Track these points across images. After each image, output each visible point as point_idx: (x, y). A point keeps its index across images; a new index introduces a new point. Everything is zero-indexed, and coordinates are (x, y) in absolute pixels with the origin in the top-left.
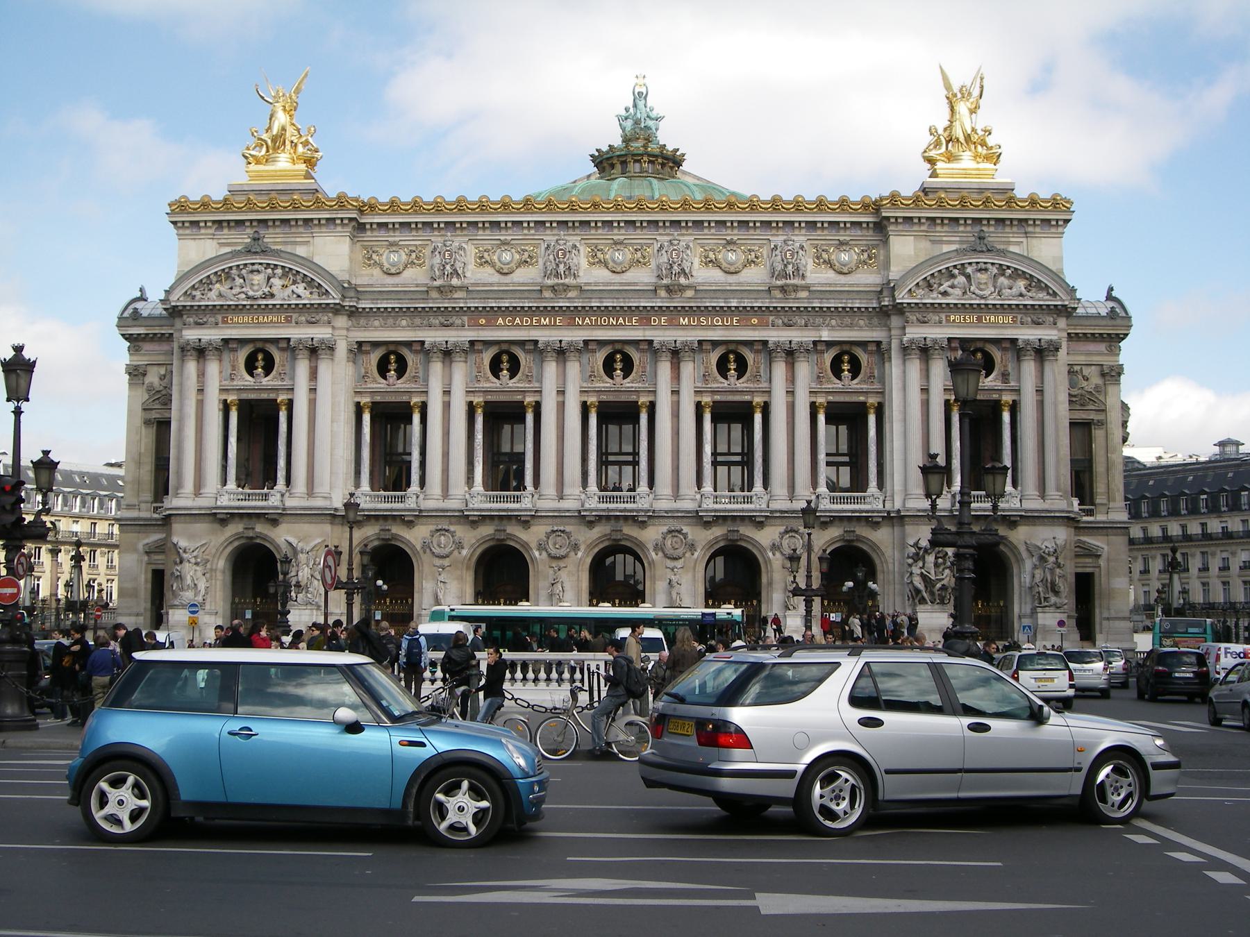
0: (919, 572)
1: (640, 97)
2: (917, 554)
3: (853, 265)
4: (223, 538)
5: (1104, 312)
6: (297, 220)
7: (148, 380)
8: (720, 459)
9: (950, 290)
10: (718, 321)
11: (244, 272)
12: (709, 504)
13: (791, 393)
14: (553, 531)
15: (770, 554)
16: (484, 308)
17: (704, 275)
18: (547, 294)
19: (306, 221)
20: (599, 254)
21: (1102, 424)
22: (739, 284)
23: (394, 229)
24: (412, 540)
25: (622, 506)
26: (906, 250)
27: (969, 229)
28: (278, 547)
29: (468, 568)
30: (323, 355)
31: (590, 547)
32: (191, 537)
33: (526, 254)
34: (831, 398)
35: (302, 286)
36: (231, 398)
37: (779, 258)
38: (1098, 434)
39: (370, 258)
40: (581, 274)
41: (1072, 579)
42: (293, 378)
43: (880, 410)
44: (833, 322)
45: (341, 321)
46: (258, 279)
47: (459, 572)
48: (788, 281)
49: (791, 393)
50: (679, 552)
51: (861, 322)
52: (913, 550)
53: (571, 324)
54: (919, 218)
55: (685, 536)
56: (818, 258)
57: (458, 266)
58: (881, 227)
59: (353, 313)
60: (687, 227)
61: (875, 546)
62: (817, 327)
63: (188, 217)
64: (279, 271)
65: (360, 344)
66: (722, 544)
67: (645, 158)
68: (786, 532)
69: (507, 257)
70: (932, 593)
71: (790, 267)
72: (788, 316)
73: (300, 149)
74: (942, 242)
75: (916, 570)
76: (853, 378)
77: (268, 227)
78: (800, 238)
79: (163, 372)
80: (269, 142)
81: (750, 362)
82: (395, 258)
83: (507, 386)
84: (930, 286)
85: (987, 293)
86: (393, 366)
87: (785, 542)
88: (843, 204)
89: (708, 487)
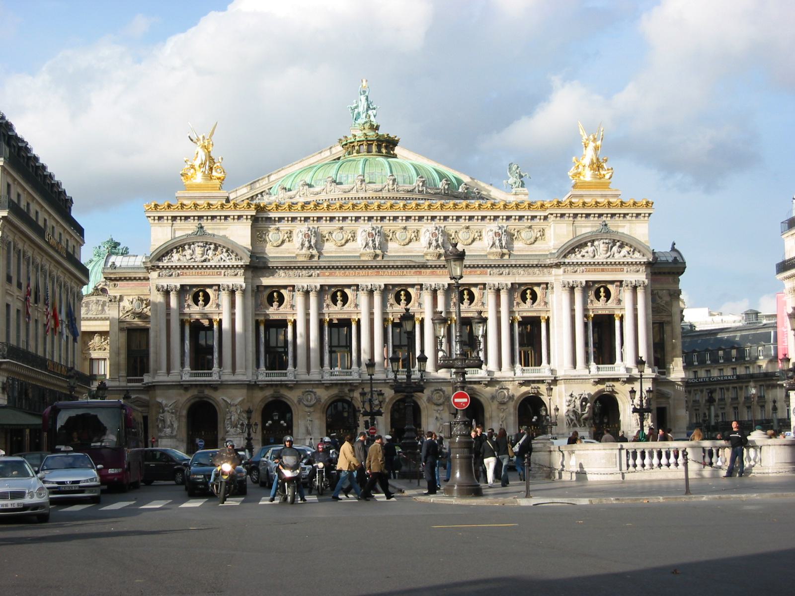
0: (572, 410)
5: (670, 260)
7: (122, 304)
9: (586, 254)
11: (192, 246)
15: (490, 401)
19: (226, 217)
21: (670, 323)
24: (292, 397)
27: (596, 219)
29: (323, 413)
35: (226, 254)
38: (667, 328)
39: (261, 238)
41: (655, 411)
45: (249, 274)
50: (441, 401)
53: (378, 275)
55: (444, 392)
58: (546, 218)
65: (258, 287)
67: (375, 143)
70: (579, 421)
74: (581, 226)
79: (131, 298)
80: (197, 167)
85: (608, 255)
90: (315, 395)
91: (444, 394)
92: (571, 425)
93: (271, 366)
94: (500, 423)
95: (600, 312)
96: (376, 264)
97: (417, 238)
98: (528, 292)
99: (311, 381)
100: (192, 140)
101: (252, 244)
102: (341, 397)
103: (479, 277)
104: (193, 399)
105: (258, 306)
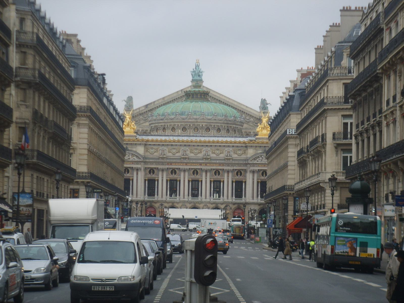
1: (197, 66)
10: (215, 165)
12: (212, 200)
13: (228, 179)
18: (182, 159)
19: (135, 144)
22: (219, 157)
26: (251, 152)
42: (133, 174)
43: (245, 182)
45: (142, 164)
55: (208, 206)
59: (145, 163)
62: (234, 166)
69: (174, 151)
72: (228, 165)
78: (231, 149)
81: (221, 173)
83: (174, 176)
89: (212, 197)
97: (201, 152)
101: (144, 154)
105: (146, 174)
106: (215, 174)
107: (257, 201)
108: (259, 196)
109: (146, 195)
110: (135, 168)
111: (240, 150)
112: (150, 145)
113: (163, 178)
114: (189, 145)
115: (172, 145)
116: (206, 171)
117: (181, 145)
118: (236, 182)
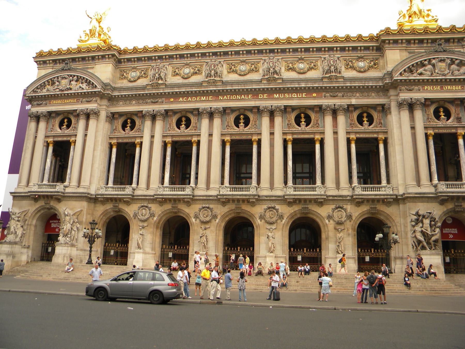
0: (420, 229)
2: (417, 220)
3: (366, 68)
4: (34, 209)
6: (88, 57)
8: (297, 175)
9: (424, 72)
10: (294, 95)
11: (60, 79)
13: (335, 133)
14: (204, 208)
15: (327, 221)
16: (173, 93)
17: (287, 75)
19: (93, 58)
20: (233, 67)
23: (134, 61)
24: (129, 212)
25: (241, 193)
28: (60, 214)
29: (157, 228)
30: (91, 117)
31: (223, 217)
32: (20, 207)
33: (196, 69)
34: (358, 136)
36: (50, 140)
37: (326, 64)
39: (123, 75)
40: (223, 77)
43: (386, 142)
44: (358, 95)
45: (105, 102)
46: (64, 82)
47: (151, 230)
48: (332, 74)
49: (335, 133)
50: (274, 219)
51: (373, 94)
52: (416, 217)
53: (217, 100)
54: (402, 40)
55: (277, 210)
56: (347, 66)
57: (162, 75)
58: (380, 49)
60: (278, 52)
61: (388, 217)
62: (350, 98)
63: (42, 59)
64: (75, 78)
65: (113, 114)
66: (299, 216)
68: (337, 208)
69: (187, 71)
70: (428, 243)
71: (332, 68)
72: (333, 91)
73: (102, 36)
75: (418, 228)
76: (370, 125)
77: (76, 62)
82: (134, 74)
84: (411, 71)
85: (446, 72)
86: (129, 125)
87: (336, 214)
88: (360, 38)
90: (149, 210)
91: (277, 212)
92: (419, 248)
93: (115, 183)
94: (338, 244)
95: (441, 131)
96: (215, 89)
98: (365, 115)
99: (147, 196)
100: (88, 16)
102: (176, 213)
103: (315, 99)
104: (43, 209)
106: (298, 122)
107: (432, 190)
108: (435, 177)
109: (111, 184)
110: (82, 110)
111: (362, 57)
112: (129, 60)
113: (153, 137)
114: (226, 53)
115: (182, 56)
116: (272, 114)
117: (204, 55)
118: (358, 141)
